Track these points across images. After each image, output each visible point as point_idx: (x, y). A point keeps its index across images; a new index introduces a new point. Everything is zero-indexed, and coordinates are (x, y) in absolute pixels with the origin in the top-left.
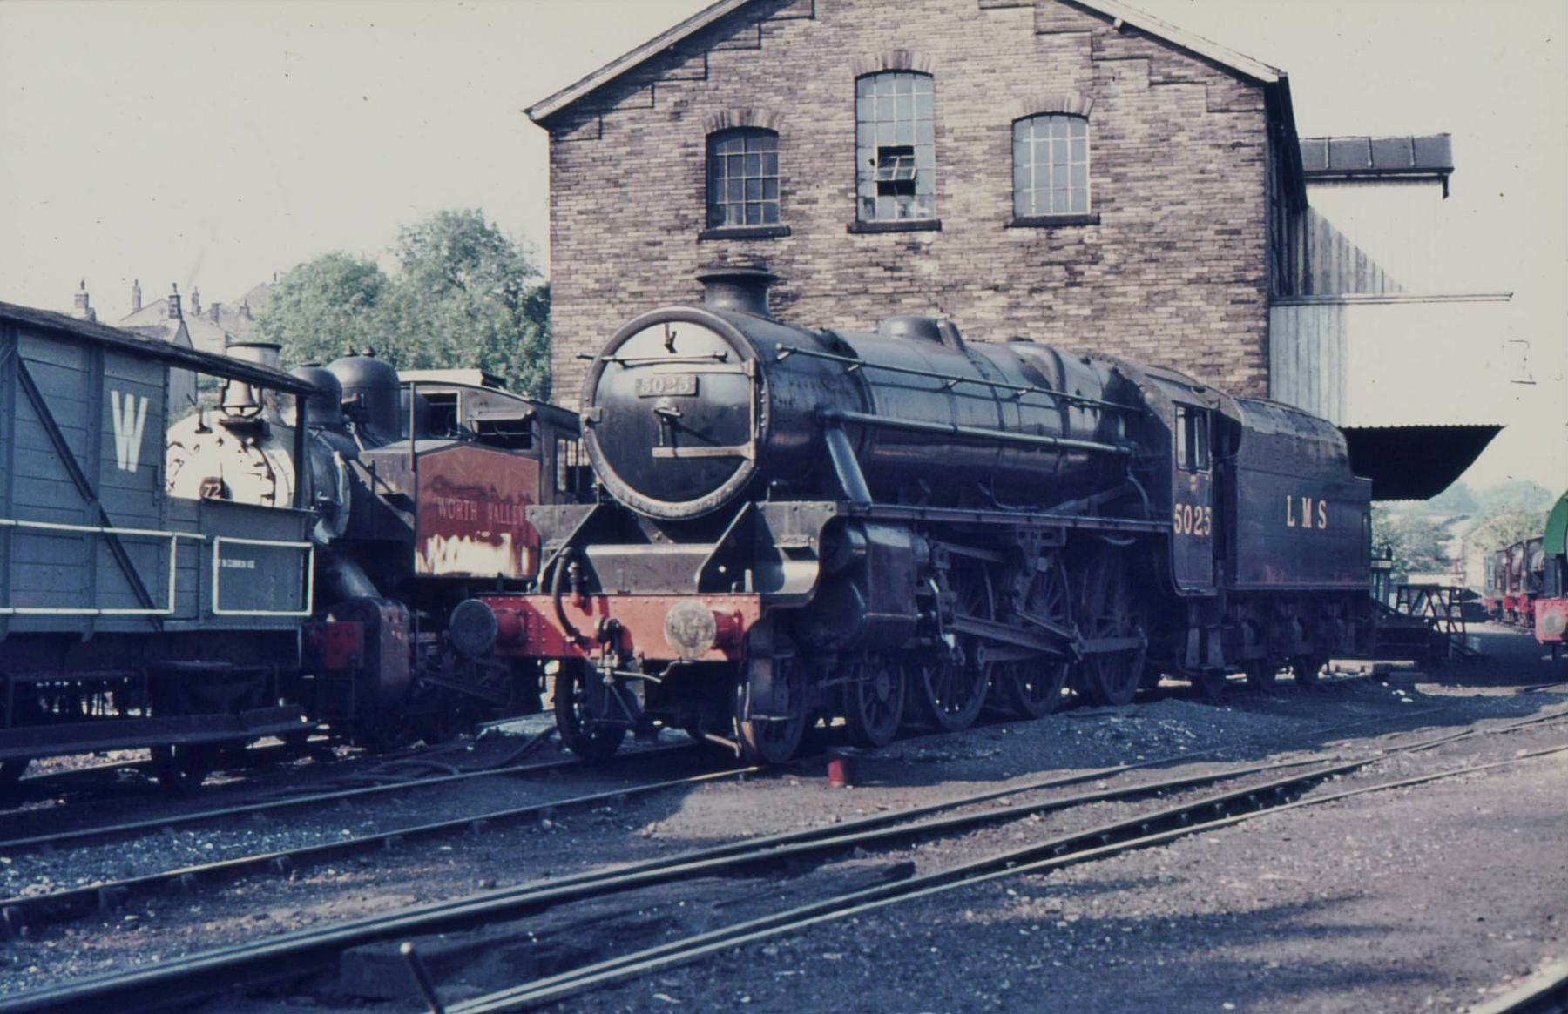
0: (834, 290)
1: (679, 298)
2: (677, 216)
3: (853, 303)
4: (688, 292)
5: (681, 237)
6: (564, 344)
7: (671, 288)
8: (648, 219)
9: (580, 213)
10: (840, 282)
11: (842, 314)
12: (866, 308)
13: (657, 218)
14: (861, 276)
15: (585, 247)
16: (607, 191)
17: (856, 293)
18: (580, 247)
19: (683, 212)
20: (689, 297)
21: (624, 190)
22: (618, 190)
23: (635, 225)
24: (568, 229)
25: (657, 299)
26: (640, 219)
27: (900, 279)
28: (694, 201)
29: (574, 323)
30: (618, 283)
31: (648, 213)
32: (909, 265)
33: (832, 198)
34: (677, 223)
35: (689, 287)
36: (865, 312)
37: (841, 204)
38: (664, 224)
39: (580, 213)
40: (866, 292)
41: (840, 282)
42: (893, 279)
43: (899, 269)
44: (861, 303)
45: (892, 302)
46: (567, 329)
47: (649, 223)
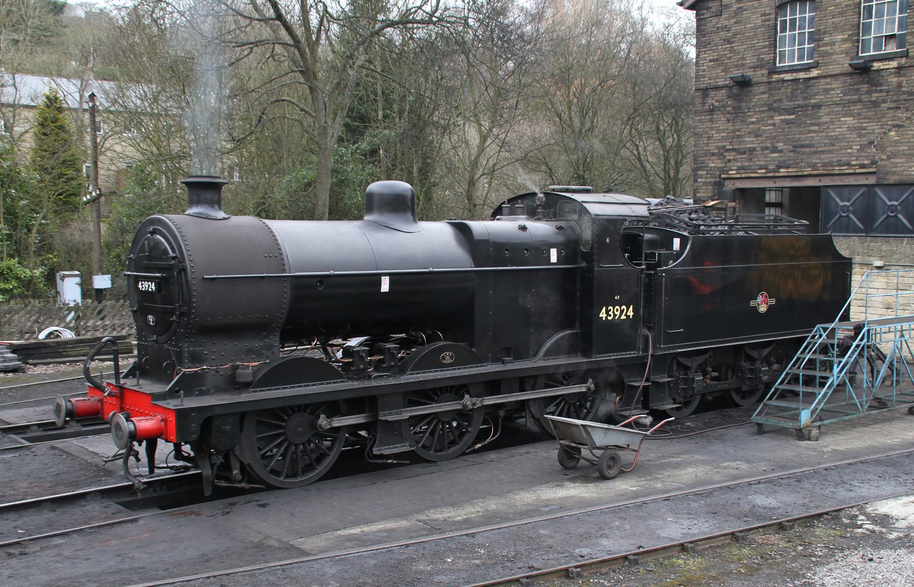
0: (841, 100)
1: (757, 110)
2: (758, 59)
3: (852, 108)
4: (762, 106)
5: (760, 72)
7: (754, 104)
8: (744, 62)
9: (710, 61)
10: (844, 95)
11: (845, 116)
12: (859, 111)
13: (748, 61)
14: (858, 90)
15: (712, 81)
16: (724, 47)
17: (854, 102)
18: (709, 82)
19: (761, 57)
20: (763, 109)
21: (733, 45)
22: (729, 46)
23: (736, 66)
24: (704, 71)
25: (746, 111)
26: (740, 62)
27: (881, 91)
28: (767, 49)
29: (705, 126)
30: (727, 102)
31: (743, 59)
32: (887, 82)
33: (844, 41)
34: (759, 63)
35: (763, 102)
36: (859, 114)
37: (848, 45)
38: (752, 64)
39: (710, 61)
40: (860, 101)
41: (844, 95)
42: (877, 92)
43: (881, 85)
44: (856, 108)
45: (875, 107)
46: (702, 130)
47: (743, 65)
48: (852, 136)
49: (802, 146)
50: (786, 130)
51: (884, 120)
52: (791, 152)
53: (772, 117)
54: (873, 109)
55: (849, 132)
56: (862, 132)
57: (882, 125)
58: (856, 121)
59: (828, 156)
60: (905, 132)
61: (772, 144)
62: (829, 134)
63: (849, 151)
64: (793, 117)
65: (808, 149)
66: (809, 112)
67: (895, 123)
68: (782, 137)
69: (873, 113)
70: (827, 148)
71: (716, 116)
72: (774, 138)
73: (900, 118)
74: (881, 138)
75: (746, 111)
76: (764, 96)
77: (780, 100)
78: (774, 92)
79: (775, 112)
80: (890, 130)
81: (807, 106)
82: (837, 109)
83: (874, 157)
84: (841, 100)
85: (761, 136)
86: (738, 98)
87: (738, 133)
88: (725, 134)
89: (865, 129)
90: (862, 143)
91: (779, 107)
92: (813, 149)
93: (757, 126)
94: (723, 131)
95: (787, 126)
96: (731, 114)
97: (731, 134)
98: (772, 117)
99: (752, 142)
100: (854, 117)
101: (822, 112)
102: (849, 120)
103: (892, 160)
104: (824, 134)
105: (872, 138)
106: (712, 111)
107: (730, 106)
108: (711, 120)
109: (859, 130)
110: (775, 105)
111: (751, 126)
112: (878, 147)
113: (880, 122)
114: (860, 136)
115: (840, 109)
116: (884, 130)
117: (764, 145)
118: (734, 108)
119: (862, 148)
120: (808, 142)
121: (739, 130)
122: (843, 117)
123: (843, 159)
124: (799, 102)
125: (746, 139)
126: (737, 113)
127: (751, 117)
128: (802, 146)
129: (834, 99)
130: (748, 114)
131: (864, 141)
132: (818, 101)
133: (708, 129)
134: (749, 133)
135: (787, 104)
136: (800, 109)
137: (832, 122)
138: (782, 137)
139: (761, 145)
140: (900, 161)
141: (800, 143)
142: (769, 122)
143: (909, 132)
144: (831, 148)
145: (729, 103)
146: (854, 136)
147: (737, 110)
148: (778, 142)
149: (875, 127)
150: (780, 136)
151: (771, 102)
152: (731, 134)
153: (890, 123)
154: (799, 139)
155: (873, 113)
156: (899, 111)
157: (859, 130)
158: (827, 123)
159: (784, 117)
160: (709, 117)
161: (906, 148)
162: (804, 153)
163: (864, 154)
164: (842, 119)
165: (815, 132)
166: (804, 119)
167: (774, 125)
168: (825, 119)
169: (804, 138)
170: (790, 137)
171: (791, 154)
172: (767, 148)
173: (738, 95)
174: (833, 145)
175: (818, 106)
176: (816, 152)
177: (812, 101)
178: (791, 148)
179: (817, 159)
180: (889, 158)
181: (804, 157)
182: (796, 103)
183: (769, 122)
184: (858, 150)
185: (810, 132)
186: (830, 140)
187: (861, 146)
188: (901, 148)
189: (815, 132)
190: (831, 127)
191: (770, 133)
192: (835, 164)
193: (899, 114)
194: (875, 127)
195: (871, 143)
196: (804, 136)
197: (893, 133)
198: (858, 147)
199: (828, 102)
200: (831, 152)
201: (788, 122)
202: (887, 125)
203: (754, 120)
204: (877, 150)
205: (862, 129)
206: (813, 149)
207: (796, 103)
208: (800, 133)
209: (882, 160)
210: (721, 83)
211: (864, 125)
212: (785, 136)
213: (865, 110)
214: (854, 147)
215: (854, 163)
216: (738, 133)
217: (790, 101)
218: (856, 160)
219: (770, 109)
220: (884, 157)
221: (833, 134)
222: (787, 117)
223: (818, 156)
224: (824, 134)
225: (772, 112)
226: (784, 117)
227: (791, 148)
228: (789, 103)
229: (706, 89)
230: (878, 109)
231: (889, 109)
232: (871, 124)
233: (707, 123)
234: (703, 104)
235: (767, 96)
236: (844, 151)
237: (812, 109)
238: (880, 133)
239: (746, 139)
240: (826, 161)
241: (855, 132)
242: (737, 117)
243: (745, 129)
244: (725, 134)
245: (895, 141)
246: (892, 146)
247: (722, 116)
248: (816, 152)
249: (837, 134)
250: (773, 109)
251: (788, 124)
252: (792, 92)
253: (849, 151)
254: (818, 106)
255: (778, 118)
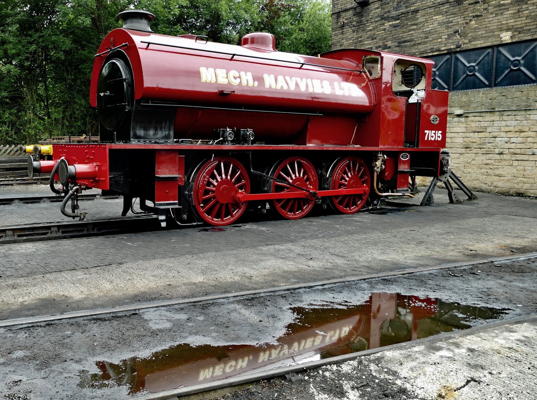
0: (434, 4)
1: (373, 21)
3: (441, 8)
6: (335, 47)
7: (371, 17)
11: (436, 14)
12: (447, 10)
15: (343, 6)
18: (341, 7)
20: (376, 20)
25: (366, 22)
35: (377, 15)
36: (446, 12)
46: (336, 41)
48: (442, 29)
49: (405, 42)
50: (393, 32)
51: (466, 13)
52: (397, 46)
53: (383, 24)
54: (457, 7)
55: (439, 27)
56: (449, 25)
57: (464, 17)
58: (444, 17)
59: (423, 46)
60: (483, 20)
61: (383, 43)
62: (424, 30)
63: (439, 40)
64: (398, 21)
65: (409, 43)
66: (409, 17)
67: (474, 14)
68: (390, 37)
69: (457, 10)
70: (423, 40)
71: (346, 30)
72: (385, 39)
73: (479, 10)
74: (464, 27)
75: (366, 22)
76: (377, 10)
77: (389, 11)
78: (385, 6)
79: (385, 20)
80: (471, 21)
81: (408, 12)
82: (429, 11)
83: (459, 42)
84: (434, 4)
85: (376, 38)
86: (359, 15)
87: (360, 39)
88: (351, 41)
89: (452, 22)
90: (449, 33)
91: (388, 17)
92: (412, 43)
93: (373, 32)
94: (350, 39)
95: (394, 29)
96: (355, 26)
97: (355, 41)
98: (383, 24)
99: (370, 44)
100: (443, 14)
101: (419, 15)
102: (439, 18)
103: (472, 43)
104: (421, 31)
105: (457, 28)
106: (343, 26)
107: (355, 21)
108: (342, 33)
109: (447, 24)
110: (386, 15)
111: (369, 33)
112: (461, 34)
113: (463, 15)
114: (448, 28)
115: (433, 10)
116: (466, 21)
117: (378, 45)
118: (357, 22)
119: (449, 37)
120: (409, 38)
121: (361, 37)
122: (434, 16)
123: (435, 47)
124: (403, 11)
125: (366, 42)
126: (360, 26)
127: (369, 26)
128: (405, 42)
129: (428, 4)
130: (367, 25)
131: (451, 31)
132: (416, 7)
133: (341, 39)
134: (368, 38)
135: (394, 13)
136: (403, 15)
137: (427, 21)
138: (390, 37)
139: (375, 45)
140: (479, 42)
141: (403, 40)
142: (381, 28)
143: (486, 20)
144: (426, 40)
145: (354, 19)
146: (443, 29)
147: (360, 23)
148: (387, 41)
149: (459, 20)
150: (388, 37)
151: (382, 14)
152: (355, 41)
153: (470, 15)
154: (402, 37)
155: (457, 10)
156: (478, 5)
157: (447, 24)
158: (422, 22)
159: (391, 23)
160: (340, 31)
161: (484, 32)
162: (406, 47)
163: (450, 41)
164: (434, 18)
165: (414, 30)
166: (406, 22)
167: (384, 30)
168: (421, 20)
169: (406, 36)
170: (396, 36)
171: (397, 49)
172: (380, 47)
173: (360, 13)
174: (427, 38)
175: (416, 11)
176: (415, 45)
177: (412, 8)
178: (396, 44)
179: (415, 49)
180: (470, 41)
181: (406, 49)
182: (400, 11)
183: (381, 28)
184: (446, 38)
185: (410, 31)
186: (425, 34)
187: (448, 35)
188: (480, 33)
189: (414, 30)
190: (425, 25)
191: (382, 36)
192: (429, 51)
193: (478, 7)
194: (459, 20)
195: (456, 32)
196: (406, 34)
197: (473, 22)
198: (446, 37)
199: (423, 7)
200: (425, 43)
201: (395, 26)
202: (468, 16)
203: (371, 28)
204: (461, 36)
205: (449, 23)
206: (412, 43)
207: (400, 11)
208: (404, 32)
209: (464, 43)
210: (349, 6)
211: (451, 19)
212: (392, 36)
213: (452, 8)
214: (443, 37)
215: (443, 49)
216: (360, 39)
217: (396, 11)
218: (445, 46)
219: (382, 19)
220: (467, 41)
221: (427, 29)
222: (394, 22)
223: (416, 47)
224: (421, 31)
225: (383, 21)
226: (391, 23)
227: (396, 44)
228: (395, 12)
229: (339, 12)
230: (462, 6)
231: (469, 4)
232: (456, 18)
233: (340, 36)
234: (337, 23)
235: (380, 10)
236: (435, 41)
237: (412, 14)
238: (463, 24)
239: (366, 42)
240: (422, 50)
241: (444, 26)
242: (359, 28)
243: (365, 35)
244: (351, 41)
245: (476, 27)
246: (472, 32)
247: (350, 29)
248: (415, 45)
249: (430, 29)
250: (383, 18)
251: (395, 27)
252: (397, 4)
253: (439, 40)
254: (416, 11)
255: (387, 25)
